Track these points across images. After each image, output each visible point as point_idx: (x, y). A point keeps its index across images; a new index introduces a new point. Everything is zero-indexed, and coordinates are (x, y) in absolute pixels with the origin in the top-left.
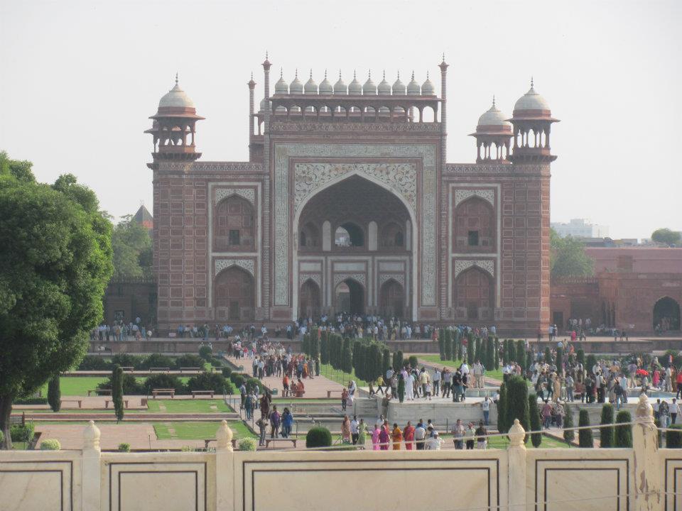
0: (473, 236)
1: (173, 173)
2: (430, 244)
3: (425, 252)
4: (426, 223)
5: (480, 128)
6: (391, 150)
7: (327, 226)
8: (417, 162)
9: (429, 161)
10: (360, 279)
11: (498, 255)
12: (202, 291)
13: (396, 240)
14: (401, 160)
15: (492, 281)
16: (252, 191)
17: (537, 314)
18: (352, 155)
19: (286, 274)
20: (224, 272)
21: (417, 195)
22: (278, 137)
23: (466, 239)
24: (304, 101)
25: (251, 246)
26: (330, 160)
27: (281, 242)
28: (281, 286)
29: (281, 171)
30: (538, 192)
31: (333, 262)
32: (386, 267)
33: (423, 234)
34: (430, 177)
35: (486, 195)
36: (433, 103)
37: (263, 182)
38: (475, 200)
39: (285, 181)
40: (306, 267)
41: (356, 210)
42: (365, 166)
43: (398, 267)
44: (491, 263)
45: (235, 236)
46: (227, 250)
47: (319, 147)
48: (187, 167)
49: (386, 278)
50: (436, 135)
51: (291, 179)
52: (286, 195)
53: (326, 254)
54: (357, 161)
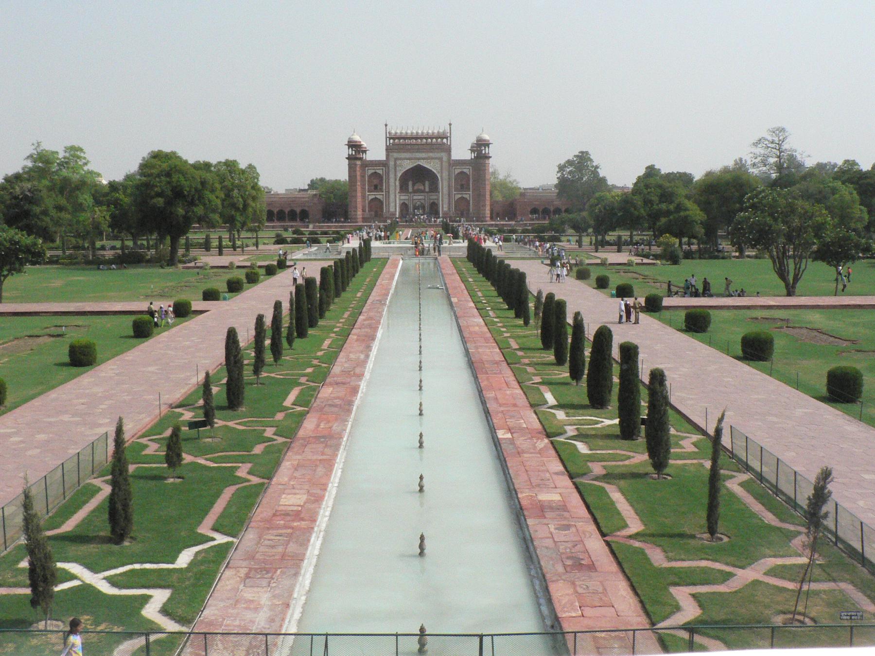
0: (462, 186)
5: (472, 147)
6: (431, 154)
7: (410, 183)
8: (441, 159)
9: (445, 159)
13: (434, 188)
14: (436, 158)
15: (468, 202)
19: (394, 201)
24: (399, 138)
25: (381, 190)
27: (392, 189)
28: (392, 205)
29: (392, 163)
33: (443, 186)
34: (445, 164)
40: (402, 198)
41: (419, 176)
43: (435, 197)
48: (359, 163)
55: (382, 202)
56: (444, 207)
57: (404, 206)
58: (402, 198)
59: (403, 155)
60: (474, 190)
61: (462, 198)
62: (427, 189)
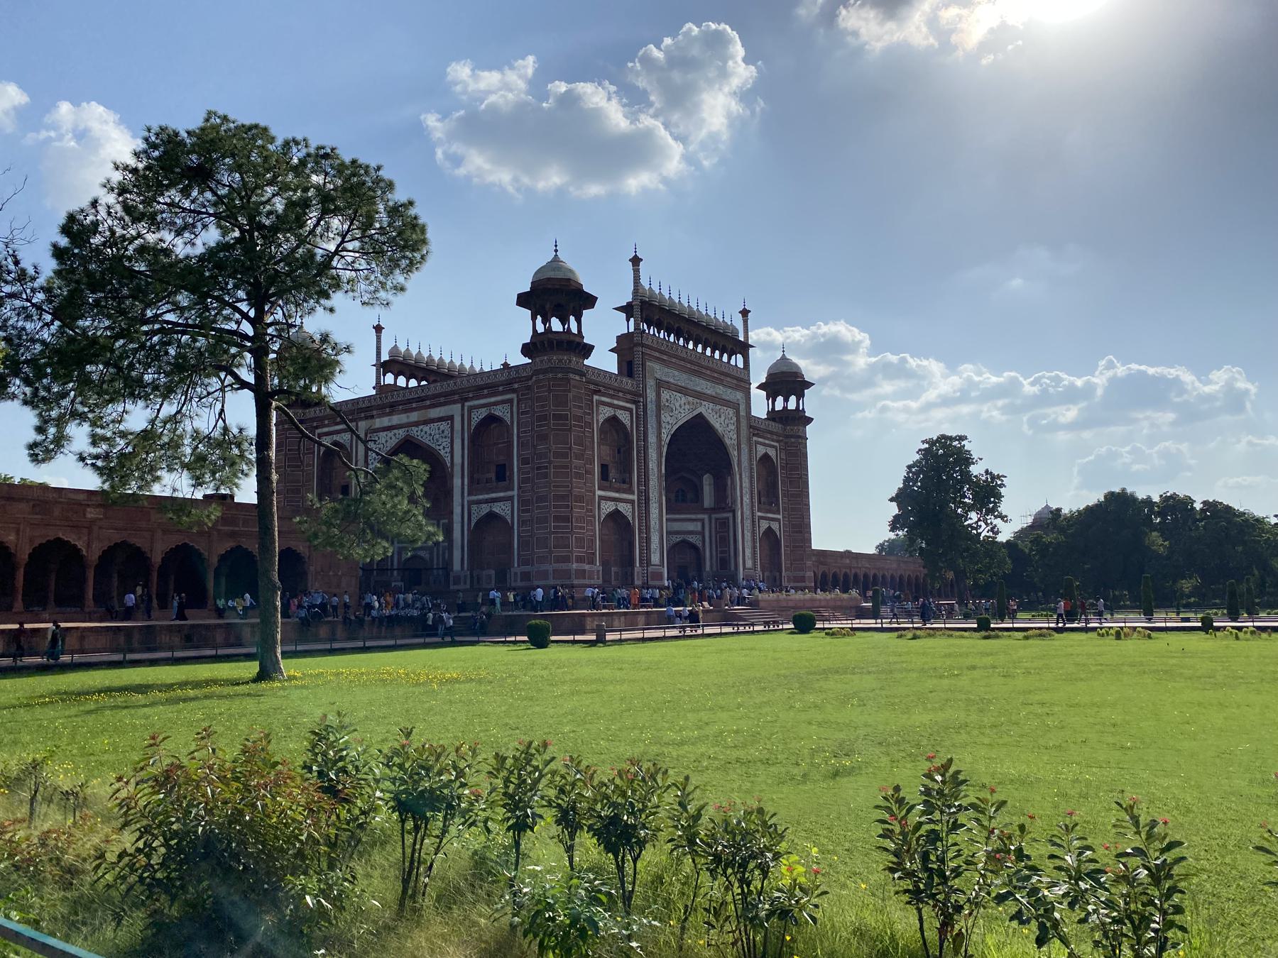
2: (746, 499)
6: (719, 390)
8: (735, 407)
9: (742, 407)
11: (780, 517)
14: (727, 403)
15: (778, 542)
18: (698, 389)
22: (648, 351)
26: (683, 391)
28: (655, 539)
29: (651, 395)
35: (772, 453)
47: (676, 373)
49: (678, 538)
50: (741, 381)
51: (659, 408)
60: (784, 509)
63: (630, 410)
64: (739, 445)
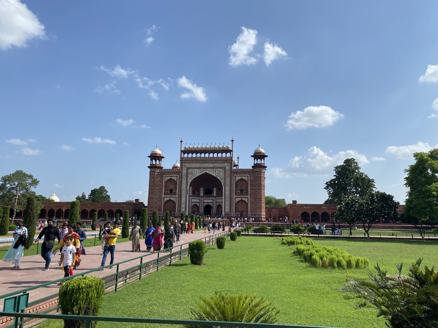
0: (242, 191)
1: (152, 172)
2: (228, 193)
3: (226, 195)
4: (227, 186)
6: (216, 165)
7: (202, 189)
8: (224, 168)
10: (211, 204)
11: (249, 196)
12: (160, 207)
14: (219, 168)
16: (176, 177)
17: (261, 215)
20: (167, 201)
21: (224, 178)
23: (240, 192)
26: (199, 168)
27: (184, 192)
28: (183, 206)
29: (184, 171)
30: (261, 177)
31: (203, 199)
32: (218, 201)
33: (226, 190)
34: (228, 173)
36: (230, 151)
37: (179, 174)
38: (242, 179)
39: (185, 174)
40: (193, 200)
42: (209, 170)
43: (220, 201)
44: (247, 199)
45: (171, 190)
46: (168, 195)
49: (218, 204)
52: (185, 178)
53: (201, 197)
54: (206, 168)
55: (175, 203)
56: (226, 208)
57: (195, 208)
58: (193, 200)
59: (193, 165)
60: (251, 194)
61: (242, 200)
62: (215, 195)
63: (177, 176)
64: (225, 178)
